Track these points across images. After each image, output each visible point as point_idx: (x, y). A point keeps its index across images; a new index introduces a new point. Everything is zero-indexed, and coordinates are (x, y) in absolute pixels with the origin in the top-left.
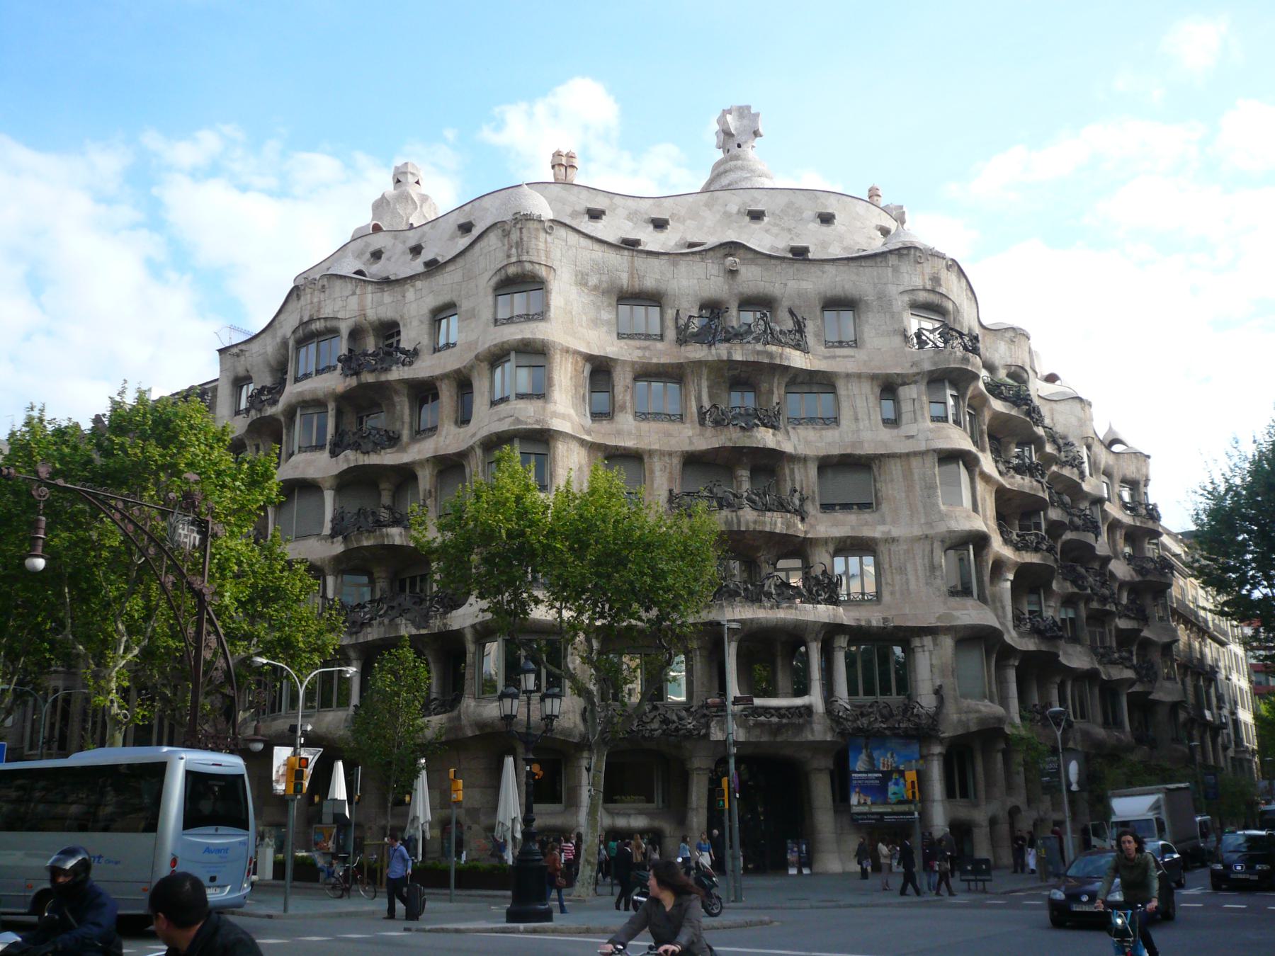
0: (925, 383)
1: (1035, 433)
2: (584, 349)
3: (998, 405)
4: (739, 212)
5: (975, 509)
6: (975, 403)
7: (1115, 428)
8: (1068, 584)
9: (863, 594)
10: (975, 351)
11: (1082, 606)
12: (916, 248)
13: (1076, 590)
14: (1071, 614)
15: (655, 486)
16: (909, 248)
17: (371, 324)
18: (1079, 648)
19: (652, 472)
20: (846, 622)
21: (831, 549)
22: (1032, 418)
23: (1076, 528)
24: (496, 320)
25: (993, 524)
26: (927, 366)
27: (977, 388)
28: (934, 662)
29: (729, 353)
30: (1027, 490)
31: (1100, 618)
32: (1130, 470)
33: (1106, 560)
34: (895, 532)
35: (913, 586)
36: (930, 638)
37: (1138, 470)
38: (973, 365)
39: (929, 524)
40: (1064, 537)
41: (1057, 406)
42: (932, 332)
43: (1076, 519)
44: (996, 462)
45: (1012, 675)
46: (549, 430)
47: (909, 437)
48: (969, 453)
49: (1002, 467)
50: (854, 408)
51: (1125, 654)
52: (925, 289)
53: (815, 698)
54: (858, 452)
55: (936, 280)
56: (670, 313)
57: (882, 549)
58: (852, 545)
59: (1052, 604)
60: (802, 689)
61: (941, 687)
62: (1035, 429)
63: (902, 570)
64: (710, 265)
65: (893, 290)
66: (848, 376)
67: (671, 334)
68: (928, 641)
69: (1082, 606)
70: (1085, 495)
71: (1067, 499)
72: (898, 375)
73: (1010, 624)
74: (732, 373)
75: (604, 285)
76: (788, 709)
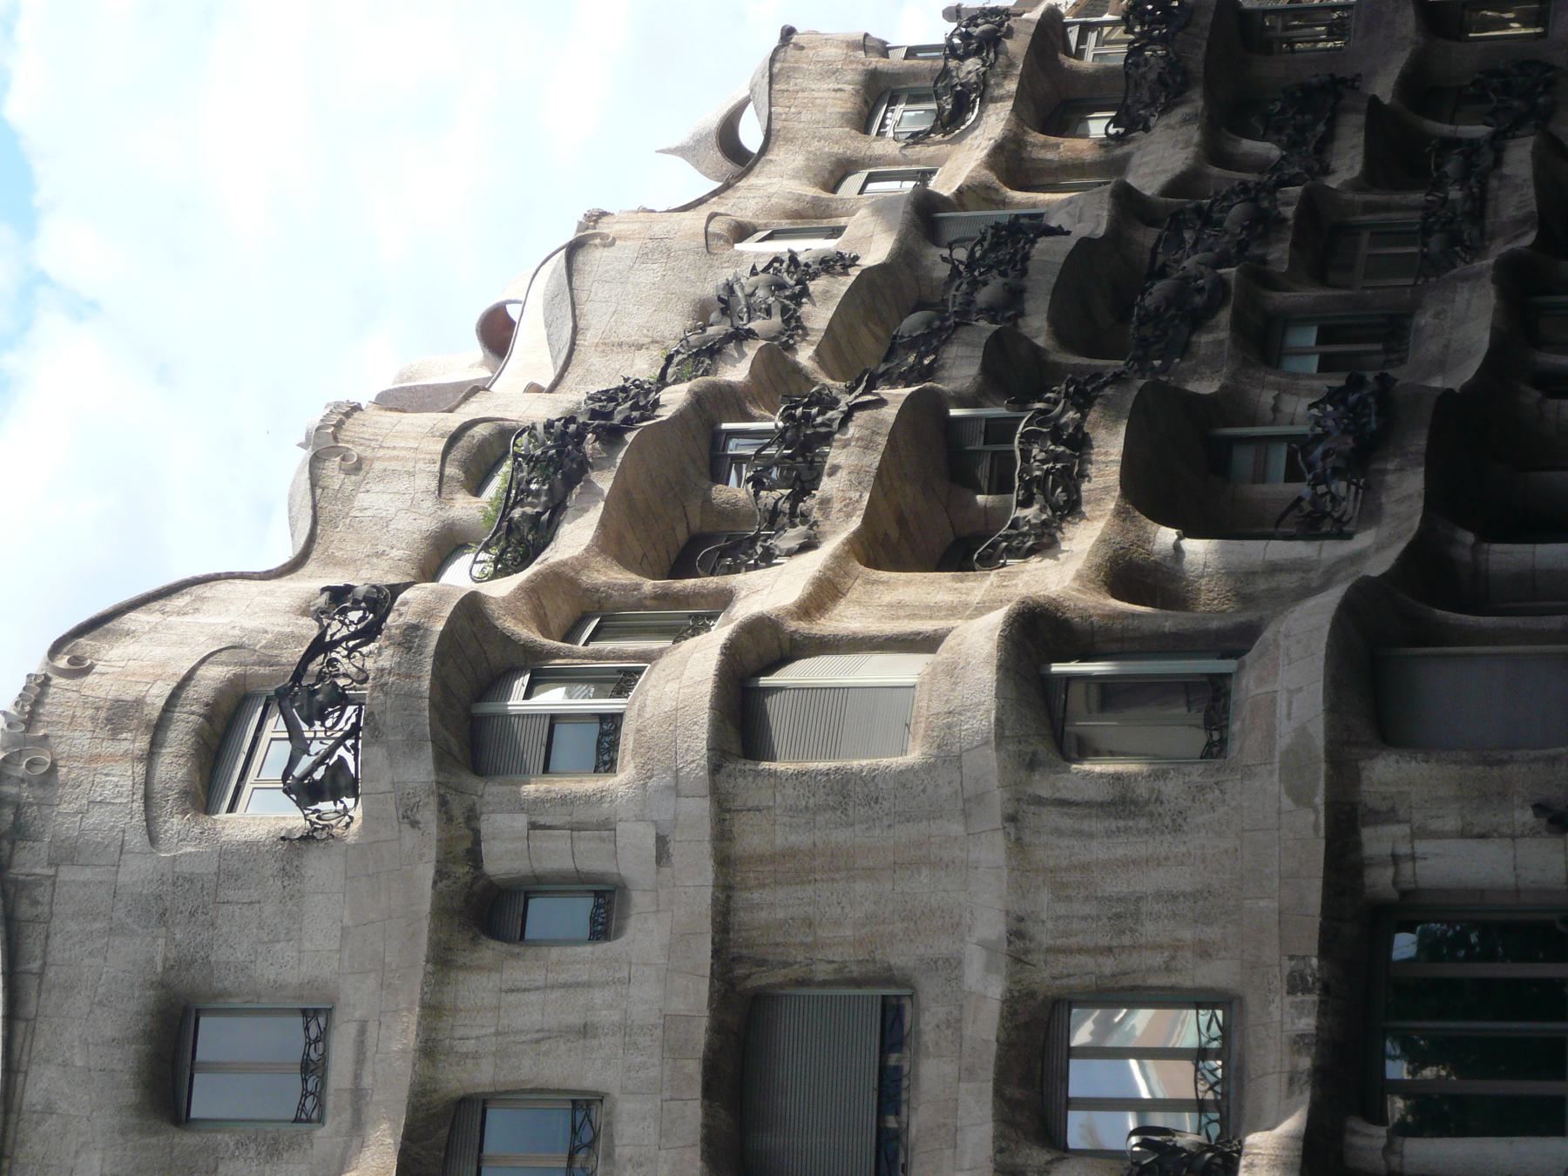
1: (680, 417)
3: (575, 537)
5: (926, 643)
6: (561, 613)
7: (682, 137)
8: (1204, 339)
9: (1200, 1054)
10: (380, 601)
11: (1278, 299)
13: (1225, 316)
14: (1307, 337)
18: (1424, 320)
20: (1293, 1123)
21: (1036, 1156)
22: (628, 423)
23: (1014, 298)
25: (980, 586)
26: (420, 771)
27: (508, 603)
28: (1451, 823)
30: (874, 459)
31: (1325, 238)
32: (826, 100)
33: (1127, 202)
34: (990, 926)
35: (1181, 879)
36: (1366, 833)
37: (831, 72)
38: (429, 613)
39: (969, 805)
40: (1041, 341)
41: (596, 324)
42: (300, 746)
43: (983, 296)
44: (768, 559)
45: (1508, 556)
48: (731, 651)
49: (791, 537)
50: (544, 1036)
51: (1451, 168)
52: (150, 756)
54: (700, 1035)
55: (118, 715)
57: (1046, 976)
59: (1268, 397)
61: (1540, 808)
62: (665, 414)
63: (1125, 912)
65: (137, 871)
66: (429, 1050)
68: (1377, 841)
69: (1278, 299)
70: (904, 257)
71: (912, 323)
72: (440, 874)
73: (1333, 550)
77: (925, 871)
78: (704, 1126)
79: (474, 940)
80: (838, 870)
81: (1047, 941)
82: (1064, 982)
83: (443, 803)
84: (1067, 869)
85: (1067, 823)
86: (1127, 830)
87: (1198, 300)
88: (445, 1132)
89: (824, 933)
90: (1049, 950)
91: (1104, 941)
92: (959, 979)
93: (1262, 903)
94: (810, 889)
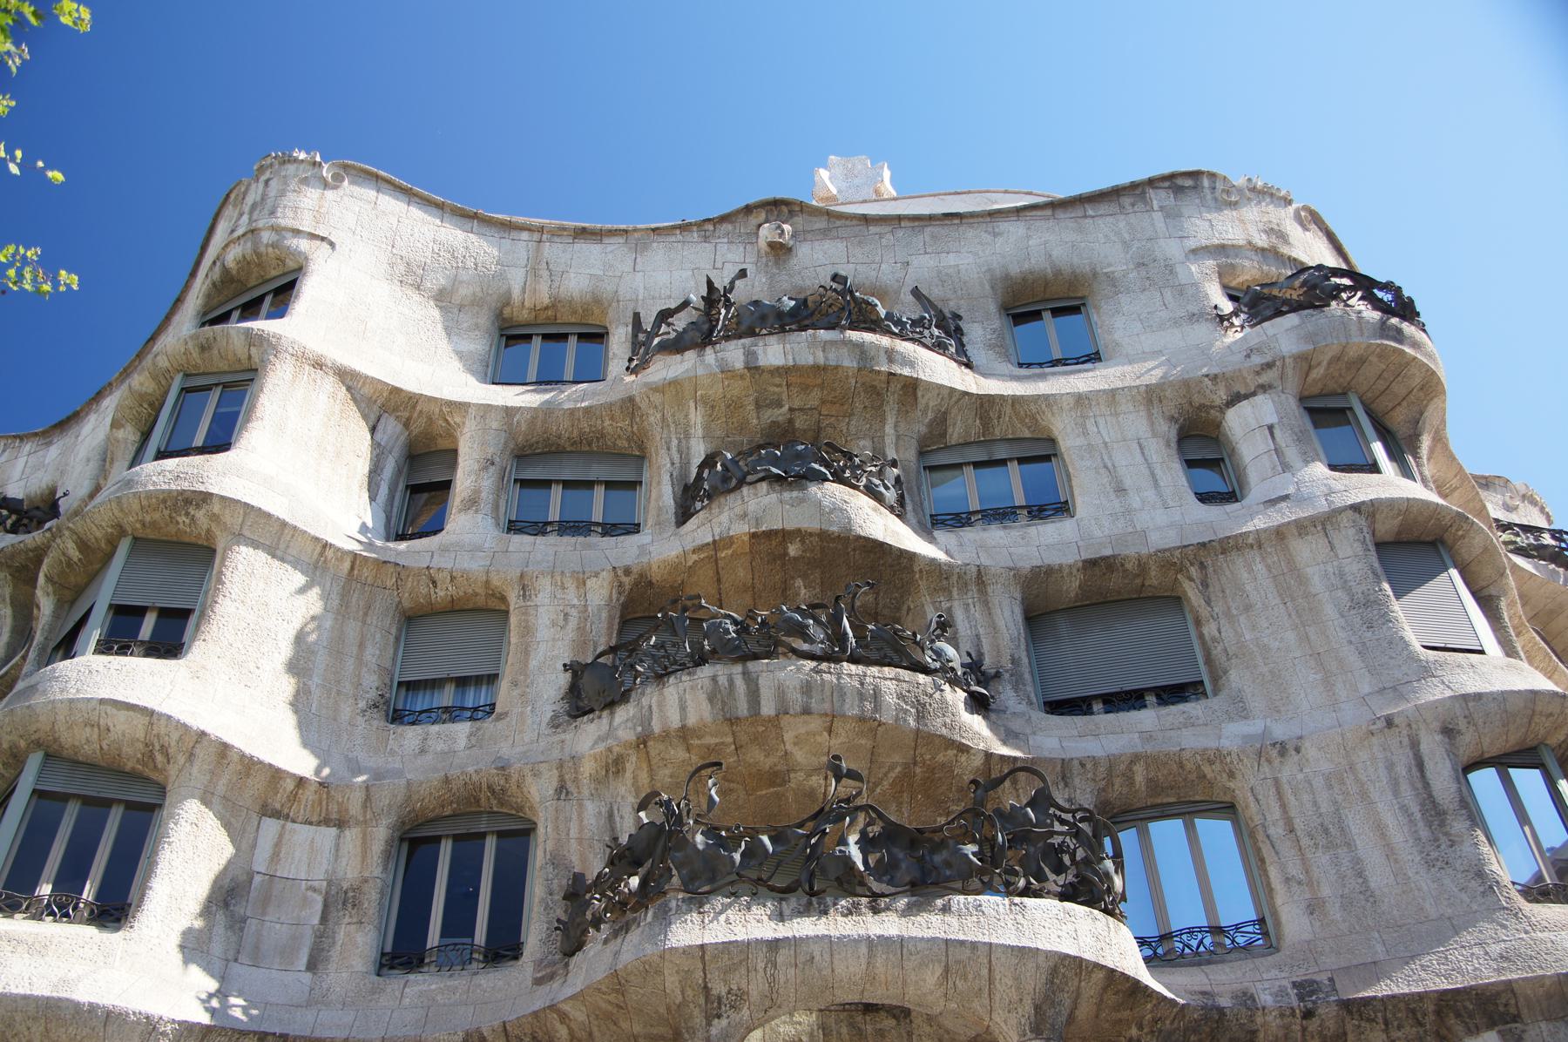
9: (1217, 930)
12: (1212, 176)
15: (533, 663)
16: (1195, 175)
19: (527, 630)
29: (750, 355)
35: (1379, 876)
46: (206, 497)
47: (1273, 502)
50: (1111, 470)
54: (1131, 550)
58: (1154, 786)
63: (1332, 835)
64: (723, 248)
65: (1172, 249)
66: (1081, 400)
72: (1214, 378)
74: (770, 415)
75: (464, 291)
77: (1318, 677)
78: (1061, 566)
79: (1172, 419)
80: (1299, 616)
81: (1285, 775)
82: (1251, 799)
83: (1269, 366)
84: (1357, 780)
85: (1401, 770)
86: (1412, 822)
88: (1027, 434)
89: (1242, 619)
90: (1277, 781)
91: (1298, 823)
92: (1231, 719)
93: (1379, 948)
94: (1278, 601)
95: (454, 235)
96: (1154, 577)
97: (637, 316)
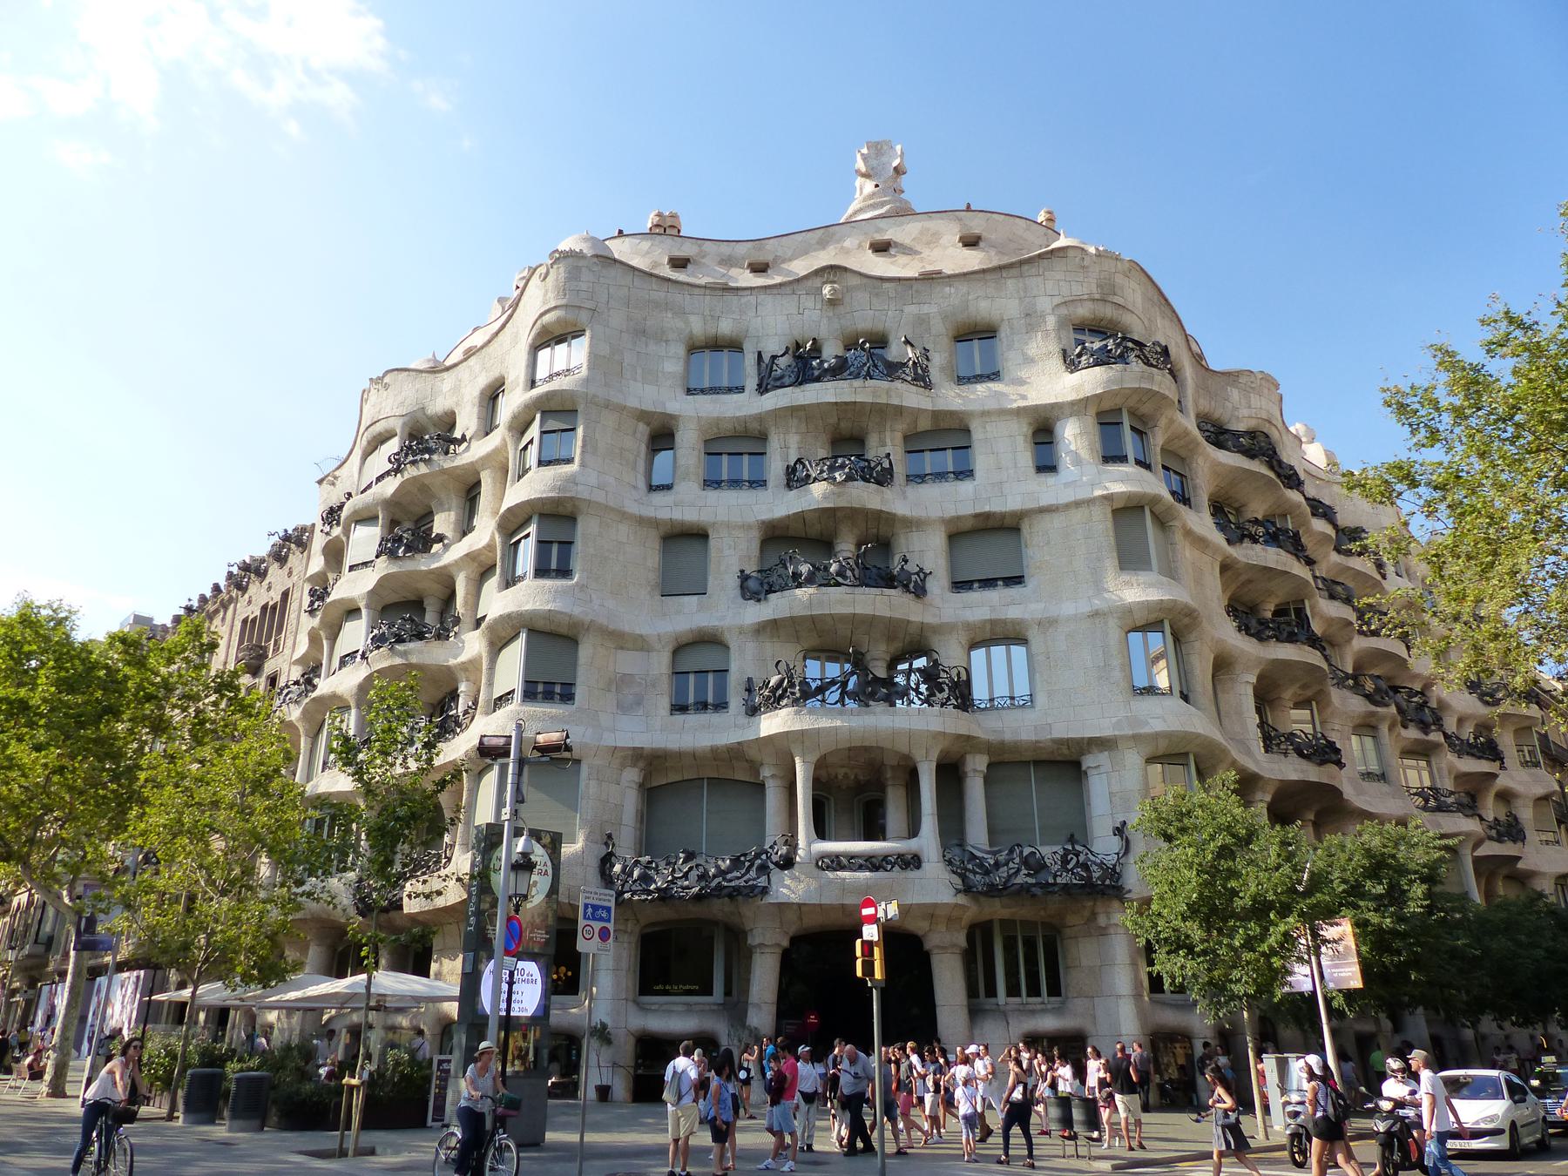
0: (1092, 411)
1: (1288, 500)
2: (633, 403)
4: (860, 246)
9: (1012, 698)
17: (430, 418)
21: (964, 638)
22: (1279, 476)
24: (533, 384)
28: (1115, 788)
53: (928, 841)
56: (750, 360)
60: (913, 831)
61: (1124, 823)
66: (985, 414)
67: (751, 383)
76: (885, 858)
87: (1378, 698)
95: (659, 294)
96: (1008, 522)
97: (760, 354)
